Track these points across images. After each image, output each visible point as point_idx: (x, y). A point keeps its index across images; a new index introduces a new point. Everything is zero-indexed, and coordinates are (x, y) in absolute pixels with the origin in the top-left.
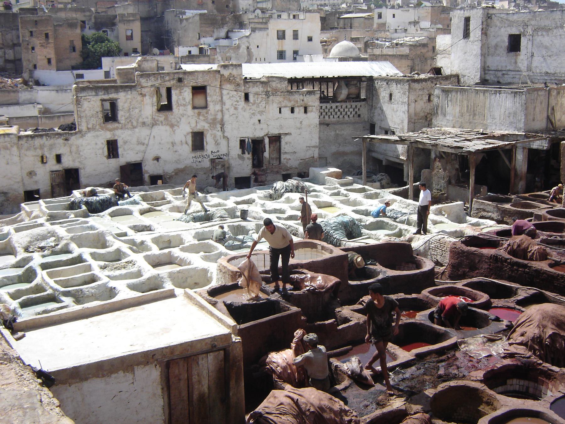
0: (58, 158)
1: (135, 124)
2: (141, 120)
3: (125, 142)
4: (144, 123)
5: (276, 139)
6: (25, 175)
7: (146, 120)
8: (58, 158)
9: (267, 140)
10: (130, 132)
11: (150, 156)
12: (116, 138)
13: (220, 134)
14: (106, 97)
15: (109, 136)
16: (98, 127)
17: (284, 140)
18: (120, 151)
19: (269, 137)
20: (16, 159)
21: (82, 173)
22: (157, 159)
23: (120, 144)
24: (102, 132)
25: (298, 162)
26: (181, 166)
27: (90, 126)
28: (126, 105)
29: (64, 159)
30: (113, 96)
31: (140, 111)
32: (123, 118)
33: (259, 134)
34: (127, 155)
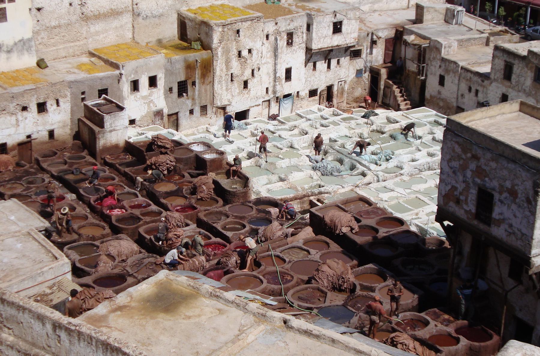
0: (477, 92)
1: (520, 88)
2: (524, 87)
4: (525, 90)
6: (459, 95)
7: (526, 89)
10: (516, 94)
12: (508, 94)
14: (508, 60)
15: (504, 90)
16: (499, 80)
20: (457, 82)
24: (501, 85)
27: (496, 77)
28: (518, 71)
29: (480, 95)
30: (511, 60)
31: (525, 80)
32: (514, 81)
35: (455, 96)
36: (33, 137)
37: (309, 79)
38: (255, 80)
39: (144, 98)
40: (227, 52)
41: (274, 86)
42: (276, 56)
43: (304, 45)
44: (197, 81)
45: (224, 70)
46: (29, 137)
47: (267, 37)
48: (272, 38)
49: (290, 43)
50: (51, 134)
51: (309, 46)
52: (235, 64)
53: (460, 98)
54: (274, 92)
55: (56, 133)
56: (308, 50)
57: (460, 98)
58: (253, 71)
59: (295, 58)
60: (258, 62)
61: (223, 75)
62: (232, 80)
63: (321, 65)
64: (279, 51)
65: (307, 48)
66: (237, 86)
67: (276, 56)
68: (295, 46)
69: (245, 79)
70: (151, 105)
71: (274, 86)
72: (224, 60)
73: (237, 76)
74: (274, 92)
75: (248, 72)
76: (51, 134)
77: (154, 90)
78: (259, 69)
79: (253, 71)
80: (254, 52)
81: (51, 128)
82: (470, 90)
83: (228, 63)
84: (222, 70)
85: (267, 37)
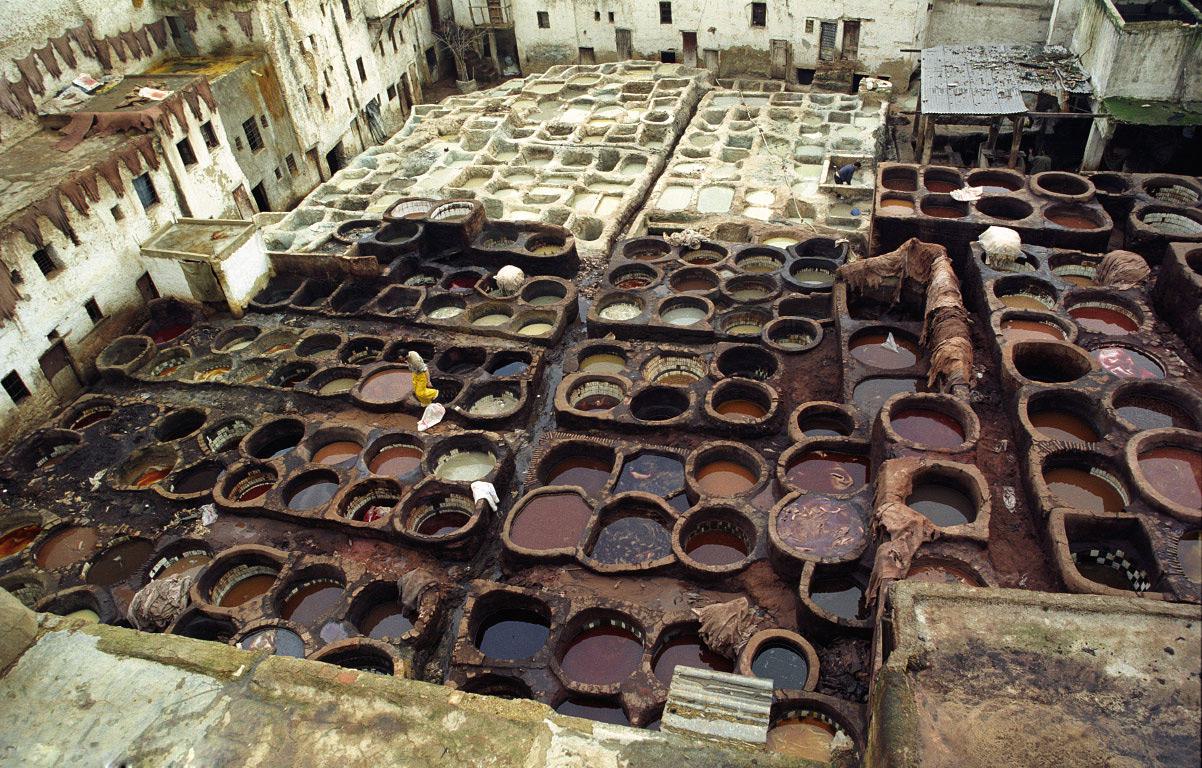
0: (611, 16)
3: (680, 6)
5: (852, 27)
8: (611, 16)
9: (841, 26)
11: (705, 27)
13: (784, 8)
17: (864, 28)
18: (673, 16)
19: (845, 22)
21: (634, 35)
22: (713, 30)
23: (673, 8)
25: (880, 62)
26: (739, 44)
33: (832, 16)
34: (682, 21)
35: (574, 35)
36: (62, 332)
37: (383, 71)
38: (333, 89)
39: (210, 171)
40: (287, 47)
41: (354, 95)
42: (340, 41)
43: (362, 16)
44: (267, 113)
45: (294, 82)
46: (53, 335)
47: (322, 6)
48: (327, 10)
49: (349, 16)
50: (91, 307)
51: (372, 13)
52: (302, 67)
53: (581, 35)
54: (357, 105)
55: (100, 303)
56: (371, 22)
57: (581, 35)
58: (325, 73)
59: (358, 41)
60: (326, 57)
61: (296, 92)
62: (309, 99)
63: (388, 46)
64: (341, 32)
65: (367, 19)
66: (316, 105)
67: (340, 41)
68: (356, 21)
69: (320, 92)
70: (224, 181)
71: (354, 95)
72: (288, 65)
73: (312, 89)
74: (357, 105)
75: (321, 76)
76: (91, 307)
77: (217, 150)
78: (331, 68)
79: (325, 73)
80: (317, 40)
81: (87, 296)
82: (597, 15)
83: (293, 64)
84: (291, 84)
85: (322, 6)
